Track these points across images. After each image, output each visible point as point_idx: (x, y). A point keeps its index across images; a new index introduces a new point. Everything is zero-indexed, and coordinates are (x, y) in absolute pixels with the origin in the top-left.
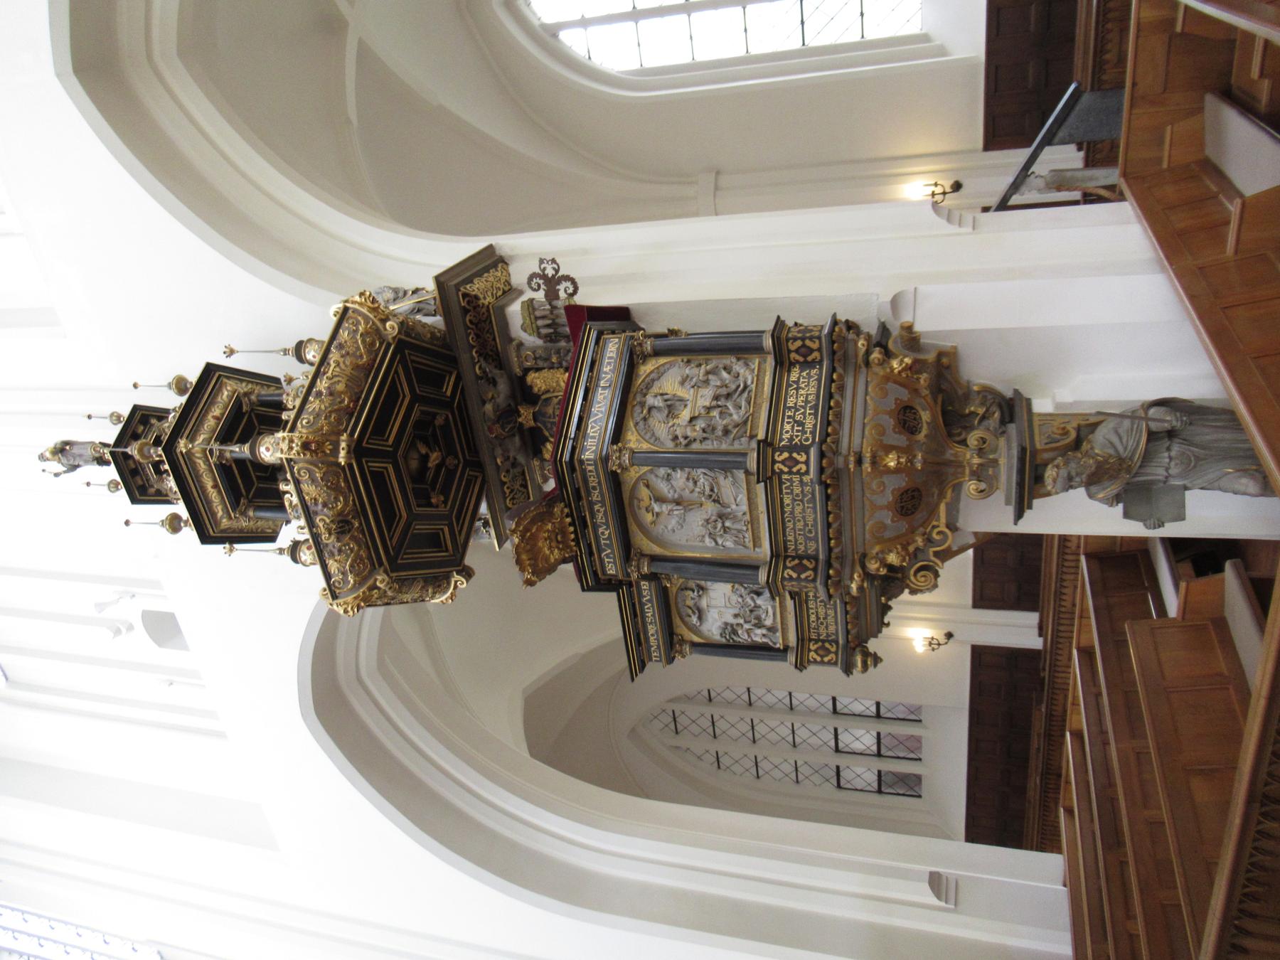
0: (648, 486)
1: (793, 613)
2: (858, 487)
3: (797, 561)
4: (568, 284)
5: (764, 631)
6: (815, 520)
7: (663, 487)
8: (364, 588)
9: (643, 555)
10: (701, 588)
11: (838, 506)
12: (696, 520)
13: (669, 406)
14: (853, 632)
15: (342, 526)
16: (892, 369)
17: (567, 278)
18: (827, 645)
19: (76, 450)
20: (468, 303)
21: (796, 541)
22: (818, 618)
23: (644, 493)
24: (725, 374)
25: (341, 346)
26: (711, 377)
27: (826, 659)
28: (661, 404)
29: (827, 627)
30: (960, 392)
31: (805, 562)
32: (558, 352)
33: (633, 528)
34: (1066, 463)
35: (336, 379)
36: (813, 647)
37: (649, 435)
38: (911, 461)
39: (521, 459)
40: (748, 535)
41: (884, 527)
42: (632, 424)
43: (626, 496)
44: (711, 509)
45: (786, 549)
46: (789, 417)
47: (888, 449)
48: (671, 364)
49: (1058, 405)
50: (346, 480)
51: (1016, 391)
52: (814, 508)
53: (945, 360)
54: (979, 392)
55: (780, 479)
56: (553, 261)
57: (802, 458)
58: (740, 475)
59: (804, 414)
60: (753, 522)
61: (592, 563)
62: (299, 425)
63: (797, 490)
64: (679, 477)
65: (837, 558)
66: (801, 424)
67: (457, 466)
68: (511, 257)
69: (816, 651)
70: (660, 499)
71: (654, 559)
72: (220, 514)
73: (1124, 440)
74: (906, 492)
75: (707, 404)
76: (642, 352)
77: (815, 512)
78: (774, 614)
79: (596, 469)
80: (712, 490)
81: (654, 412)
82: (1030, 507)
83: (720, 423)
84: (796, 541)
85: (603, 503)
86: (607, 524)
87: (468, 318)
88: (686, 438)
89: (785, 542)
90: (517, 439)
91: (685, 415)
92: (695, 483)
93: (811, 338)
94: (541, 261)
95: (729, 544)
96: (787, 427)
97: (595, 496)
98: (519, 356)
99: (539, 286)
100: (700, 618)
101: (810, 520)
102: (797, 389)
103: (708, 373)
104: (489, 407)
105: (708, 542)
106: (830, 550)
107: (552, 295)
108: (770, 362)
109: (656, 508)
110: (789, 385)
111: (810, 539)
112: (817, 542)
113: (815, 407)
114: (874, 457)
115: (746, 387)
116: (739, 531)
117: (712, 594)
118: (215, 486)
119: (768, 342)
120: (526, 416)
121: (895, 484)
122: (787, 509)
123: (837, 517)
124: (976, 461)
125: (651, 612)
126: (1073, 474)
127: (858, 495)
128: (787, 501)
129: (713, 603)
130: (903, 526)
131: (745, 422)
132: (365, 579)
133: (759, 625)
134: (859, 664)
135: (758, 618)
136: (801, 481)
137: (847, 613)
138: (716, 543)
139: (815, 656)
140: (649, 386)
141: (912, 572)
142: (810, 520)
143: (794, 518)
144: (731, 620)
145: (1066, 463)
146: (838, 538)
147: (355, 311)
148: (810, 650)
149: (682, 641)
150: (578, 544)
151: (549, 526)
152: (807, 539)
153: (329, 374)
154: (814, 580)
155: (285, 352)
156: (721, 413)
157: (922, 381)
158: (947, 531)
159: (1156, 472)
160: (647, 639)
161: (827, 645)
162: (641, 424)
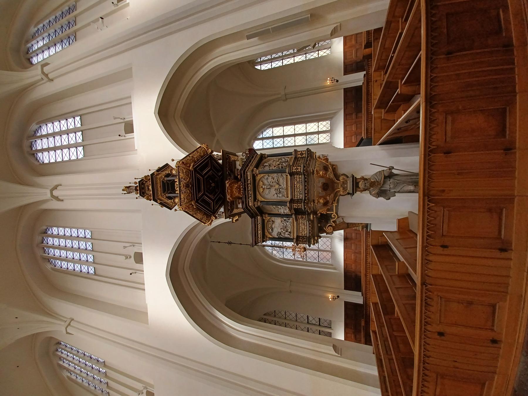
2: (313, 180)
7: (266, 182)
9: (258, 200)
12: (273, 191)
15: (187, 186)
23: (261, 183)
33: (257, 193)
40: (285, 193)
44: (277, 186)
60: (287, 189)
61: (246, 201)
71: (261, 202)
97: (249, 182)
105: (276, 195)
106: (306, 197)
119: (293, 153)
121: (322, 180)
123: (308, 187)
125: (260, 226)
130: (324, 193)
132: (189, 202)
133: (286, 231)
134: (312, 242)
146: (308, 193)
149: (267, 237)
152: (300, 194)
159: (387, 187)
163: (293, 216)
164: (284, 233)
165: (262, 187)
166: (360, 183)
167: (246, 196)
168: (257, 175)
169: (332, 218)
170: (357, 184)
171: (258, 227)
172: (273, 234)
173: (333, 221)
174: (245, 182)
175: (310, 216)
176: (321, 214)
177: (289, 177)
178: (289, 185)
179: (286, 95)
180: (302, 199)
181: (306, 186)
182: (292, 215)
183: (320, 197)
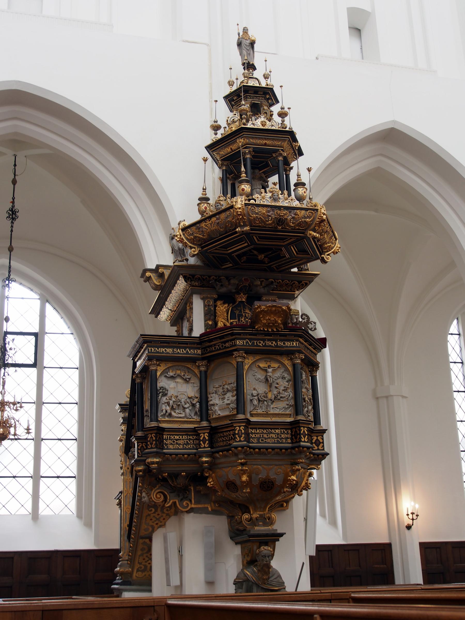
1: (180, 427)
5: (169, 411)
6: (269, 443)
7: (278, 374)
11: (277, 454)
12: (262, 389)
15: (281, 221)
20: (303, 285)
21: (257, 433)
22: (177, 440)
23: (276, 365)
29: (172, 444)
40: (260, 411)
41: (257, 474)
45: (252, 429)
52: (274, 443)
58: (288, 412)
60: (267, 415)
61: (246, 334)
63: (283, 436)
67: (240, 261)
72: (251, 140)
73: (275, 580)
74: (273, 485)
77: (272, 443)
78: (180, 417)
80: (281, 397)
84: (257, 433)
85: (277, 346)
86: (265, 346)
87: (296, 282)
89: (256, 429)
94: (315, 323)
99: (304, 319)
101: (269, 440)
111: (258, 440)
112: (257, 443)
118: (265, 145)
120: (242, 298)
121: (279, 480)
122: (273, 431)
123: (270, 453)
125: (181, 352)
127: (277, 463)
128: (277, 431)
130: (256, 482)
133: (172, 408)
136: (288, 438)
137: (183, 455)
142: (269, 440)
144: (170, 394)
151: (279, 322)
152: (258, 439)
158: (189, 508)
160: (163, 347)
165: (269, 367)
167: (255, 335)
168: (291, 359)
171: (180, 348)
173: (175, 503)
175: (206, 457)
178: (274, 419)
179: (387, 397)
182: (207, 420)
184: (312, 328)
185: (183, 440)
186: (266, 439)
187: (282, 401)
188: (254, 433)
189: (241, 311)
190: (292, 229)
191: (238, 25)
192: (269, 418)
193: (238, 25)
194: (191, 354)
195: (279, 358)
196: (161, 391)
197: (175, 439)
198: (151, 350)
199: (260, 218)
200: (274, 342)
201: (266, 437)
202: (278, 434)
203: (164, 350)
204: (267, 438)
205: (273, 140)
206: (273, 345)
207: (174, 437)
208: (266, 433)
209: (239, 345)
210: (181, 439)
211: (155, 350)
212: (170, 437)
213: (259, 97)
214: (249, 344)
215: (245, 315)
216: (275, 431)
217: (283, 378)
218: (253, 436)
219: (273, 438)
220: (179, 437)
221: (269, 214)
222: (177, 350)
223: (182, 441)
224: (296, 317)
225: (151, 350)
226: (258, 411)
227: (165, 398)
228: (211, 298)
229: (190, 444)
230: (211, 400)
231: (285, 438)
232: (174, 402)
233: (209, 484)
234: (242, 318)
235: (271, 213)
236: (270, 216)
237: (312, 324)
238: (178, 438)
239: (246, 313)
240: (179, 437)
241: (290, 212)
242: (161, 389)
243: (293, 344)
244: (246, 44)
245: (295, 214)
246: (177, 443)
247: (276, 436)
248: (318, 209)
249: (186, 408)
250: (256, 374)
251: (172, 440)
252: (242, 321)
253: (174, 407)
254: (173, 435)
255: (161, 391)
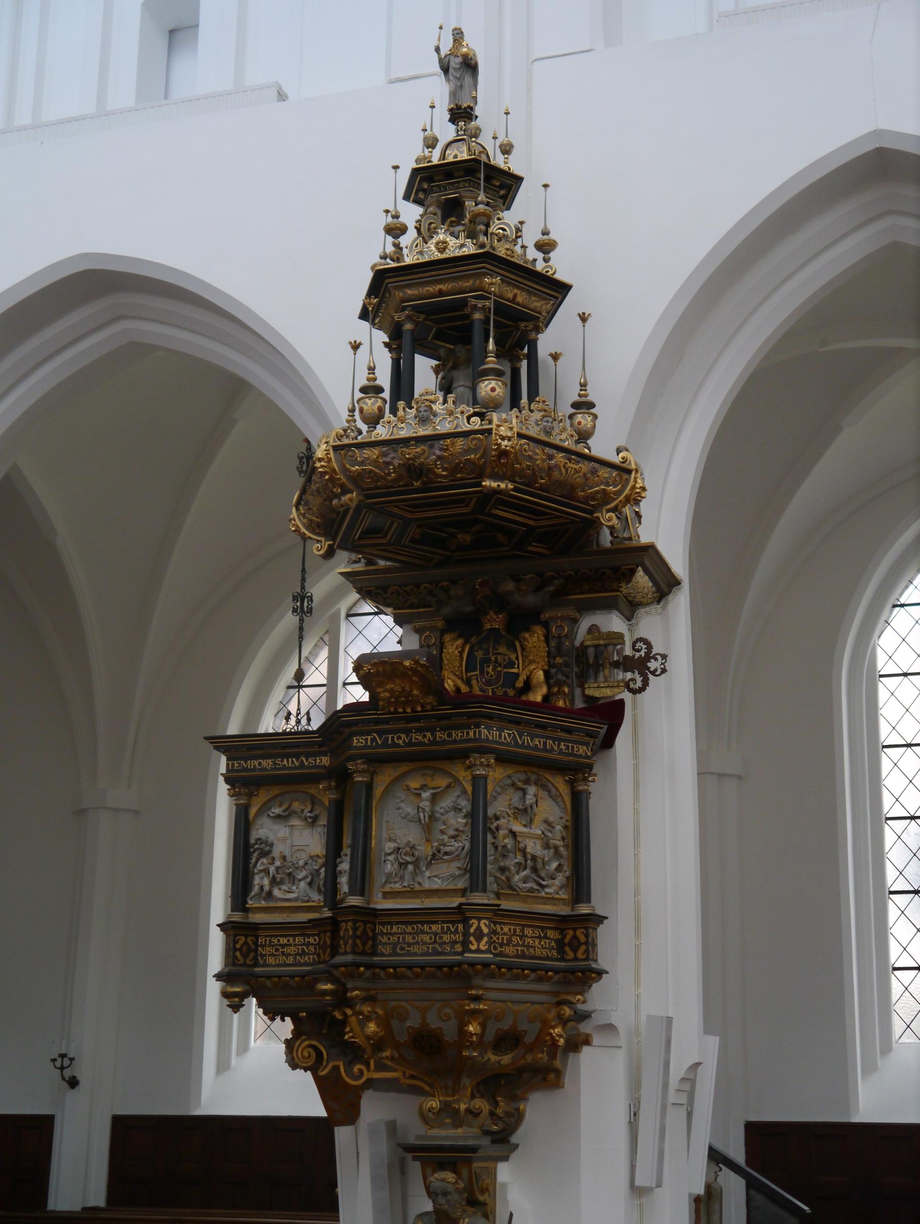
0: (448, 787)
1: (289, 920)
3: (370, 934)
4: (639, 684)
5: (267, 888)
6: (415, 954)
7: (447, 802)
8: (344, 480)
9: (373, 775)
10: (315, 819)
12: (410, 835)
13: (525, 810)
14: (268, 983)
15: (413, 470)
16: (553, 1027)
17: (646, 683)
18: (252, 955)
19: (468, 79)
21: (392, 934)
22: (283, 946)
23: (442, 782)
24: (554, 865)
25: (594, 472)
26: (552, 851)
27: (238, 954)
28: (528, 802)
29: (272, 955)
30: (518, 1092)
31: (370, 943)
32: (566, 665)
33: (404, 768)
34: (458, 1191)
35: (563, 471)
36: (249, 939)
37: (499, 790)
38: (473, 1046)
39: (447, 610)
40: (397, 887)
42: (510, 772)
43: (437, 764)
44: (425, 850)
45: (383, 924)
46: (515, 930)
47: (483, 1026)
48: (564, 809)
49: (504, 1185)
50: (462, 479)
51: (516, 1146)
52: (427, 954)
53: (552, 1076)
54: (518, 1109)
55: (458, 922)
56: (664, 671)
57: (483, 947)
58: (461, 884)
59: (518, 944)
61: (364, 722)
62: (524, 441)
63: (446, 938)
64: (460, 821)
65: (374, 974)
66: (509, 942)
68: (664, 607)
69: (246, 943)
70: (434, 799)
71: (369, 786)
72: (409, 292)
75: (529, 850)
76: (576, 780)
79: (470, 740)
80: (446, 853)
81: (520, 794)
82: (415, 1159)
83: (511, 862)
84: (392, 934)
85: (434, 742)
86: (410, 744)
87: (607, 571)
88: (497, 828)
89: (391, 924)
90: (469, 609)
91: (518, 828)
92: (453, 837)
93: (587, 951)
94: (664, 657)
95: (389, 867)
96: (506, 929)
97: (441, 735)
98: (562, 618)
100: (279, 817)
101: (414, 949)
102: (540, 937)
103: (556, 848)
104: (510, 586)
105: (389, 846)
106: (384, 968)
107: (627, 664)
108: (564, 910)
109: (426, 795)
110: (543, 928)
111: (394, 949)
112: (390, 955)
113: (523, 956)
114: (480, 1011)
115: (543, 886)
116: (402, 878)
117: (307, 832)
118: (441, 293)
119: (584, 909)
120: (494, 621)
121: (449, 1031)
124: (463, 1107)
126: (449, 1197)
128: (434, 927)
129: (296, 833)
130: (403, 1038)
131: (511, 888)
133: (274, 882)
134: (231, 989)
135: (282, 882)
136: (456, 942)
137: (292, 977)
138: (389, 854)
139: (241, 942)
140: (544, 787)
141: (314, 1042)
142: (414, 949)
143: (417, 933)
144: (276, 853)
145: (458, 1191)
146: (396, 976)
147: (628, 481)
148: (246, 936)
149: (250, 795)
150: (390, 713)
152: (395, 946)
153: (569, 465)
154: (354, 952)
155: (583, 386)
156: (519, 864)
157: (540, 1055)
158: (364, 1079)
160: (256, 758)
161: (252, 955)
162: (509, 782)
163: (327, 914)
164: (266, 871)
165: (423, 787)
166: (450, 1176)
167: (386, 721)
169: (349, 1065)
170: (451, 1165)
171: (288, 756)
172: (265, 820)
173: (336, 1068)
174: (440, 718)
175: (326, 981)
176: (345, 1022)
177: (455, 902)
180: (374, 953)
181: (423, 968)
183: (385, 1022)
184: (656, 670)
185: (295, 945)
186: (409, 945)
187: (447, 861)
188: (387, 934)
189: (487, 652)
190: (451, 481)
191: (441, 28)
192: (419, 901)
193: (441, 28)
194: (308, 767)
195: (446, 765)
196: (257, 846)
197: (281, 945)
198: (233, 765)
199: (371, 471)
200: (428, 735)
201: (411, 941)
202: (436, 934)
203: (256, 763)
204: (413, 944)
205: (454, 279)
206: (426, 740)
207: (279, 941)
208: (410, 933)
209: (357, 748)
210: (290, 945)
211: (240, 764)
212: (270, 941)
213: (458, 182)
214: (377, 742)
215: (496, 658)
216: (430, 928)
217: (457, 809)
218: (385, 940)
219: (425, 943)
220: (288, 941)
221: (387, 459)
222: (282, 761)
223: (293, 948)
224: (618, 647)
225: (233, 765)
226: (397, 886)
227: (264, 860)
228: (432, 629)
229: (309, 954)
230: (342, 862)
231: (450, 942)
232: (277, 869)
233: (346, 1037)
234: (488, 666)
235: (392, 455)
236: (388, 463)
237: (656, 659)
238: (285, 941)
239: (500, 654)
240: (288, 941)
241: (431, 447)
242: (256, 843)
243: (468, 733)
244: (461, 67)
245: (441, 449)
246: (283, 952)
247: (431, 939)
248: (491, 429)
249: (300, 880)
250: (402, 805)
251: (273, 946)
252: (488, 673)
253: (278, 880)
254: (276, 936)
255: (257, 846)
